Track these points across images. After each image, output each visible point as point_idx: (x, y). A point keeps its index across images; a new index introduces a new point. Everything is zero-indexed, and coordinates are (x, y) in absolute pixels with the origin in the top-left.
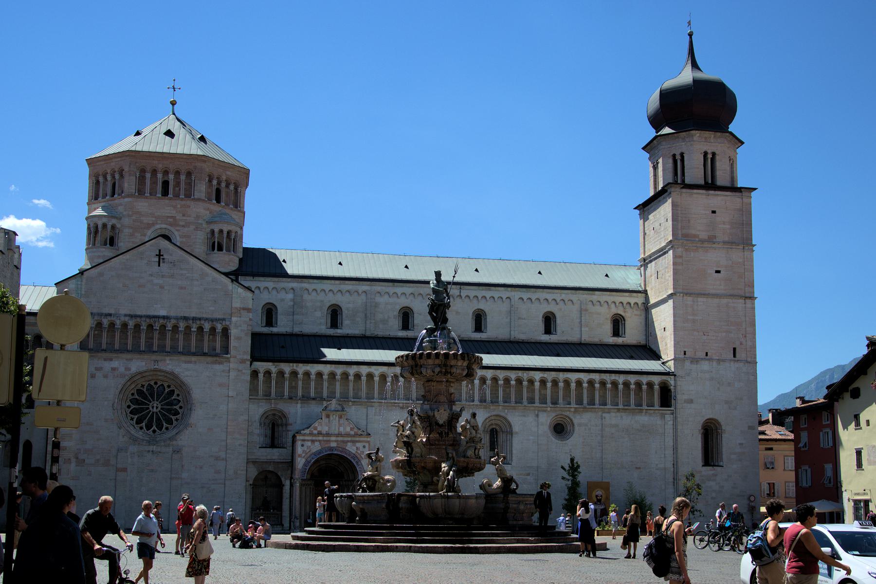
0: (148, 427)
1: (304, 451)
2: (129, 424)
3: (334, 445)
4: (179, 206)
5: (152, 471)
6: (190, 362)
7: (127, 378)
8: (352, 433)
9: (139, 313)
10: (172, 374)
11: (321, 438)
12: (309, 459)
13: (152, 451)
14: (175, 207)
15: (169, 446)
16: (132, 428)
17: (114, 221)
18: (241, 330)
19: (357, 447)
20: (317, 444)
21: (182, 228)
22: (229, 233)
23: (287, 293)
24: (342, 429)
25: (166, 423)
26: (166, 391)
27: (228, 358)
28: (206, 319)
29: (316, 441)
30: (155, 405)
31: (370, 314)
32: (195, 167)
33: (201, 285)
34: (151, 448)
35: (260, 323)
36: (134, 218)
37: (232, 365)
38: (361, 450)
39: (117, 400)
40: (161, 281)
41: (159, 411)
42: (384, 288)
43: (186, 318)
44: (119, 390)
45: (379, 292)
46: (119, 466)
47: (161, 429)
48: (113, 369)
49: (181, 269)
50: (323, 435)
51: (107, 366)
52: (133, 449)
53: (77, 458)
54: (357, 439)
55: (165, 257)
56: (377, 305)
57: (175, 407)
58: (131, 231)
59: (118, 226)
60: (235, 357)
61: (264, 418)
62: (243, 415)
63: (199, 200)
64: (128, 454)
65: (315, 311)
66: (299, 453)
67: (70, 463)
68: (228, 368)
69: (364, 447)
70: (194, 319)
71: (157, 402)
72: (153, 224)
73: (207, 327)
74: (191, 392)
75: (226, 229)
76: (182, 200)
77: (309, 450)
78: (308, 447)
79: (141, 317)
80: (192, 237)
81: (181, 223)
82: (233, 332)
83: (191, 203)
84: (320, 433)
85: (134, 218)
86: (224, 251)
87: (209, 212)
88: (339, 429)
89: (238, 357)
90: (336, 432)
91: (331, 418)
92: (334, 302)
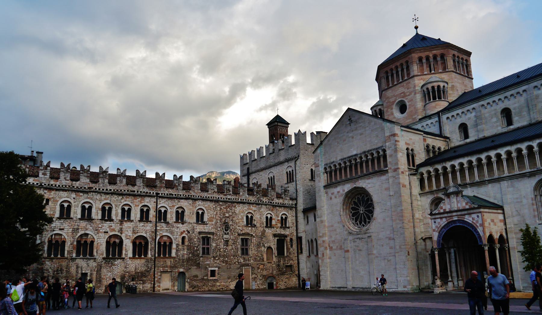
0: (361, 223)
1: (436, 227)
2: (351, 223)
3: (455, 218)
4: (405, 85)
5: (360, 250)
6: (370, 178)
7: (344, 196)
8: (467, 207)
9: (345, 157)
10: (363, 188)
11: (446, 215)
12: (441, 233)
13: (359, 238)
14: (403, 86)
15: (366, 233)
16: (352, 225)
17: (379, 107)
18: (392, 150)
19: (473, 218)
20: (444, 220)
21: (408, 97)
22: (433, 87)
23: (471, 113)
24: (459, 205)
25: (368, 219)
26: (366, 199)
27: (387, 170)
28: (374, 149)
29: (443, 217)
30: (362, 209)
31: (532, 105)
32: (409, 58)
33: (370, 128)
34: (358, 236)
35: (459, 139)
36: (386, 101)
37: (390, 174)
38: (476, 220)
39: (341, 210)
40: (350, 135)
41: (364, 212)
42: (537, 82)
43: (364, 152)
44: (342, 203)
45: (536, 87)
46: (346, 249)
47: (365, 223)
48: (338, 192)
49: (360, 123)
50: (447, 213)
51: (335, 190)
52: (351, 238)
53: (329, 246)
54: (472, 211)
55: (352, 119)
56: (537, 97)
57: (371, 208)
58: (386, 109)
59: (382, 109)
60: (391, 169)
61: (433, 206)
62: (399, 207)
63: (413, 76)
64: (349, 241)
65: (492, 118)
66: (433, 228)
67: (327, 249)
68: (388, 177)
69: (478, 216)
70: (368, 151)
71: (363, 208)
72: (395, 101)
73: (375, 155)
74: (372, 197)
75: (430, 86)
76: (406, 80)
77: (439, 226)
78: (439, 223)
79: (345, 158)
80: (414, 100)
81: (407, 94)
82: (388, 152)
83: (411, 80)
84: (445, 212)
85: (386, 101)
86: (432, 100)
87: (422, 81)
88: (457, 205)
89: (393, 168)
90: (456, 209)
91: (451, 198)
92: (504, 107)
